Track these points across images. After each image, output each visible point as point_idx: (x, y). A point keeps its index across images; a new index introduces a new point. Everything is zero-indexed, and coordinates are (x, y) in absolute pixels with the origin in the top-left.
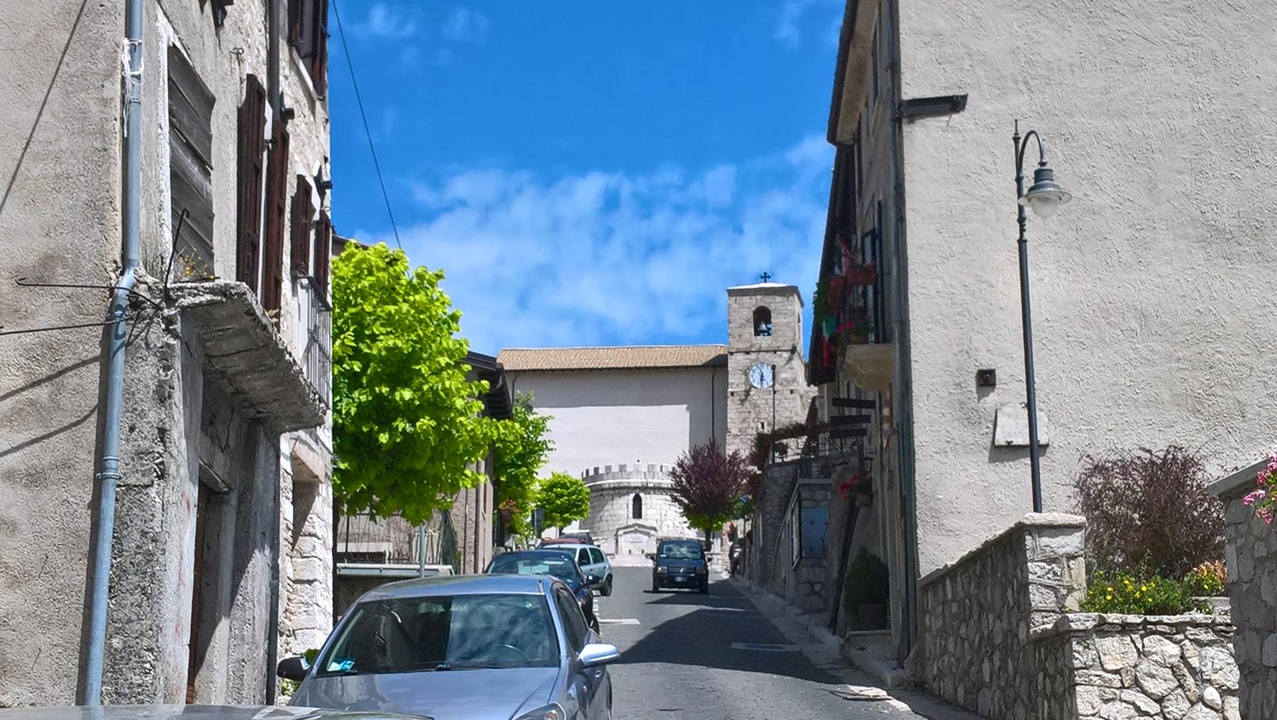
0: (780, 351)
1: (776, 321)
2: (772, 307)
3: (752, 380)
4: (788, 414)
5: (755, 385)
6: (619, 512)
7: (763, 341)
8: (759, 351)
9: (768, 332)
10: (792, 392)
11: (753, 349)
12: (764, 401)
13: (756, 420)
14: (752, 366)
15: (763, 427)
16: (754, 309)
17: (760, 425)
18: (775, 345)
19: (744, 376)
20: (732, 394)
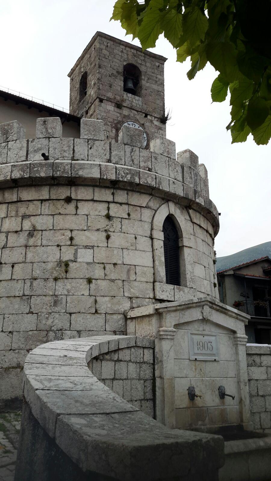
1: (148, 85)
2: (143, 69)
6: (130, 258)
7: (136, 101)
8: (131, 108)
16: (125, 63)
19: (114, 131)
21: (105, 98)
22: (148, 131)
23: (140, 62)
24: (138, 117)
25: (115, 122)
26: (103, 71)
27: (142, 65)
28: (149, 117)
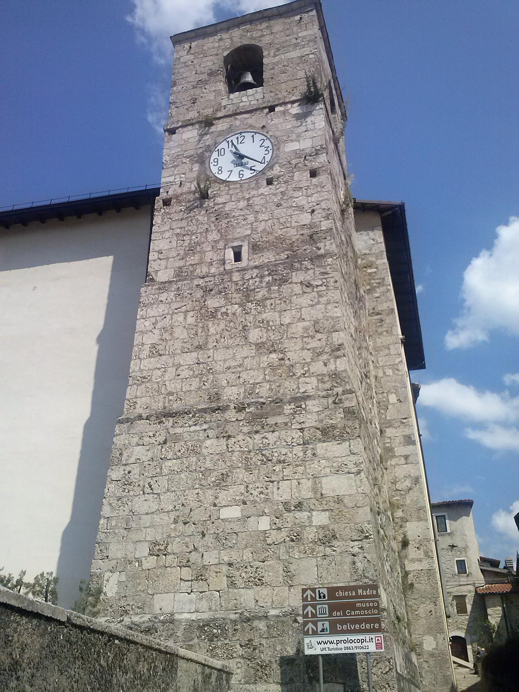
0: (285, 103)
2: (263, 43)
3: (214, 170)
4: (306, 218)
5: (223, 176)
9: (259, 82)
10: (313, 174)
11: (219, 115)
12: (242, 204)
13: (221, 245)
14: (216, 144)
15: (238, 257)
16: (226, 53)
17: (230, 254)
18: (270, 100)
19: (196, 167)
20: (167, 203)
21: (180, 124)
22: (278, 134)
23: (260, 33)
24: (250, 121)
25: (200, 151)
26: (180, 87)
27: (264, 36)
28: (277, 109)
